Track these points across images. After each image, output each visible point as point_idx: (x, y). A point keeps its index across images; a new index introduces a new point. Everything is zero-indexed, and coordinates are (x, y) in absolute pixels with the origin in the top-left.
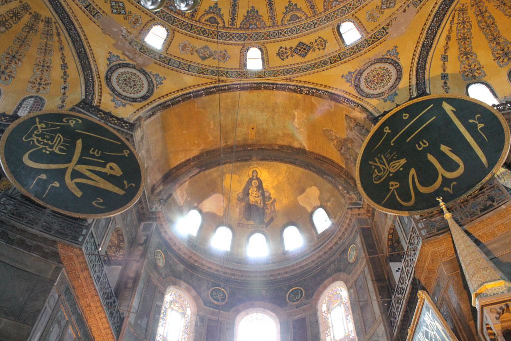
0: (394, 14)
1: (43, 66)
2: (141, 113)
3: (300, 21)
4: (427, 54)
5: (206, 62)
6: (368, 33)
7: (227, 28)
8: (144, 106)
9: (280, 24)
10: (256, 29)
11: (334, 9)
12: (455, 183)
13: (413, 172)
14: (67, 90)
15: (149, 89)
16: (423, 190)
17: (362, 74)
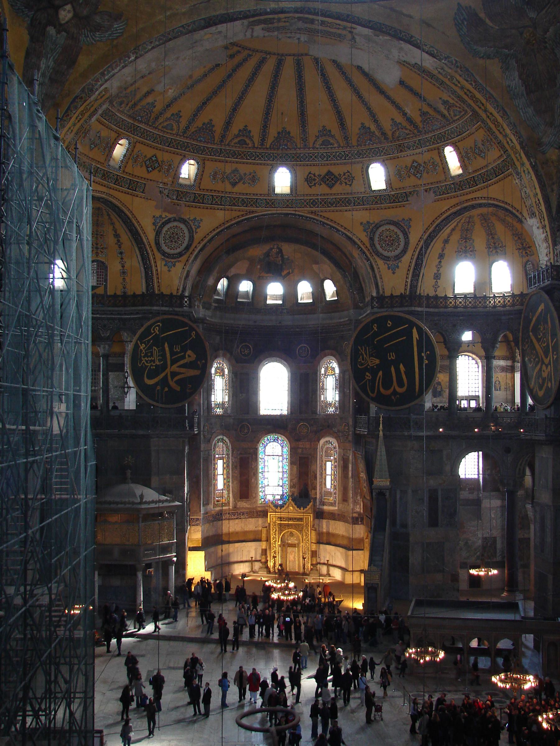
0: (417, 186)
1: (97, 234)
2: (187, 268)
3: (332, 148)
4: (432, 241)
5: (237, 189)
6: (392, 190)
7: (257, 148)
8: (189, 257)
9: (311, 145)
10: (286, 149)
11: (367, 147)
12: (398, 396)
13: (380, 373)
14: (124, 255)
15: (190, 237)
16: (382, 390)
17: (378, 228)
